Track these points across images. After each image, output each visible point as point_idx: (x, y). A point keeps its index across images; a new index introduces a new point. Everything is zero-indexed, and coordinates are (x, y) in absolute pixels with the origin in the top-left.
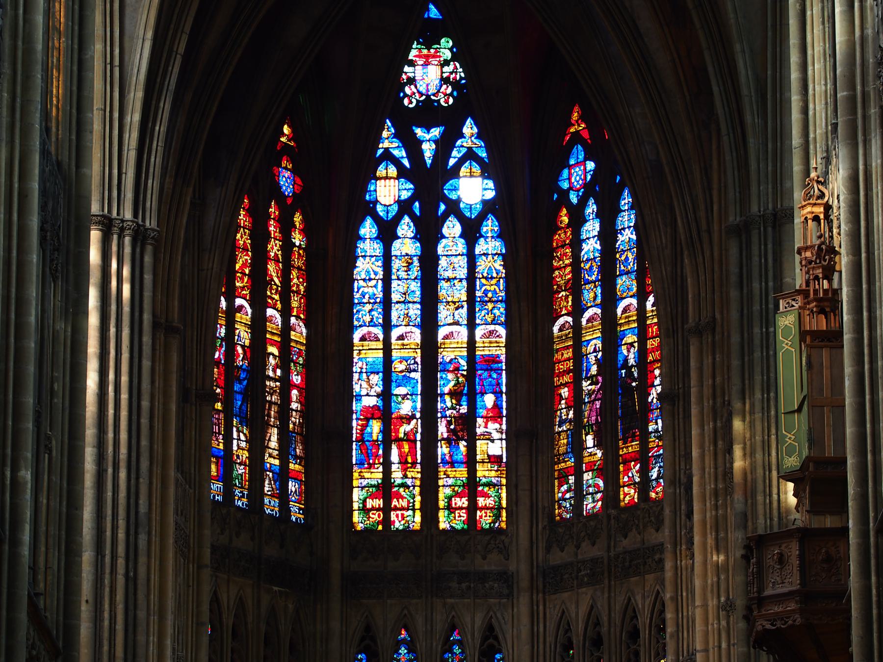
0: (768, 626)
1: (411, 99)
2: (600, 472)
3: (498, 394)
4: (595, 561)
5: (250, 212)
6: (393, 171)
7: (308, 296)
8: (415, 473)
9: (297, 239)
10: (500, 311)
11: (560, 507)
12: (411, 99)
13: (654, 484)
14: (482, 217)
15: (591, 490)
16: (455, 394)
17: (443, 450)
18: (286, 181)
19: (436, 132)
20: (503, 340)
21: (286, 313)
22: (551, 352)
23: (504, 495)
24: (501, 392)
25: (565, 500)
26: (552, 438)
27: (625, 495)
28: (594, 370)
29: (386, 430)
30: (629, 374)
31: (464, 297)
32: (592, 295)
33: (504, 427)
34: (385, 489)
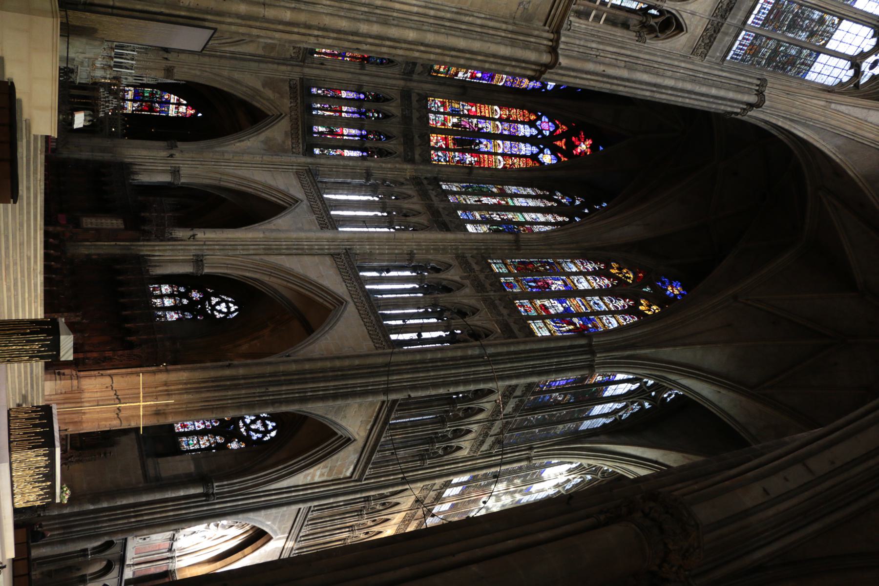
2: (443, 124)
3: (480, 79)
4: (411, 119)
11: (432, 100)
13: (436, 153)
15: (437, 118)
20: (498, 84)
22: (488, 104)
23: (442, 75)
24: (480, 80)
25: (435, 103)
26: (458, 100)
27: (434, 137)
28: (480, 126)
30: (478, 144)
32: (506, 128)
33: (467, 79)
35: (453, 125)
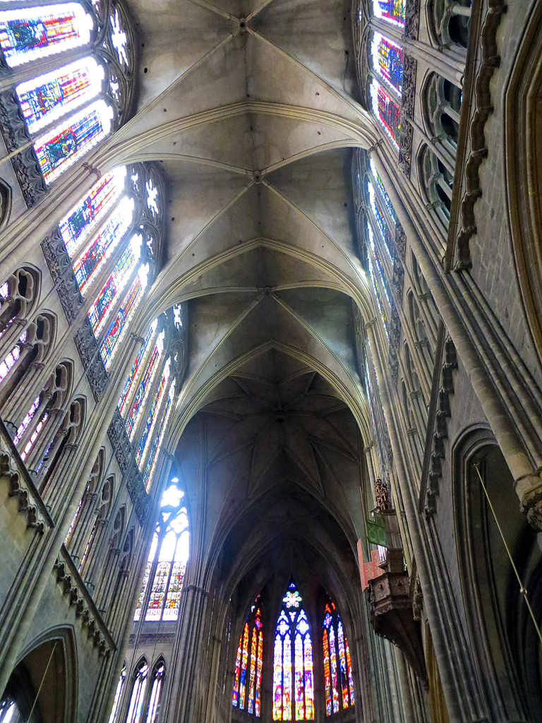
0: (380, 613)
1: (288, 606)
5: (249, 629)
6: (284, 622)
7: (263, 653)
8: (290, 703)
9: (260, 638)
10: (311, 657)
12: (288, 606)
14: (306, 634)
16: (300, 681)
17: (296, 697)
18: (258, 623)
19: (295, 613)
21: (257, 656)
22: (323, 668)
26: (325, 692)
28: (335, 671)
29: (282, 692)
31: (302, 654)
34: (282, 708)
35: (337, 691)
